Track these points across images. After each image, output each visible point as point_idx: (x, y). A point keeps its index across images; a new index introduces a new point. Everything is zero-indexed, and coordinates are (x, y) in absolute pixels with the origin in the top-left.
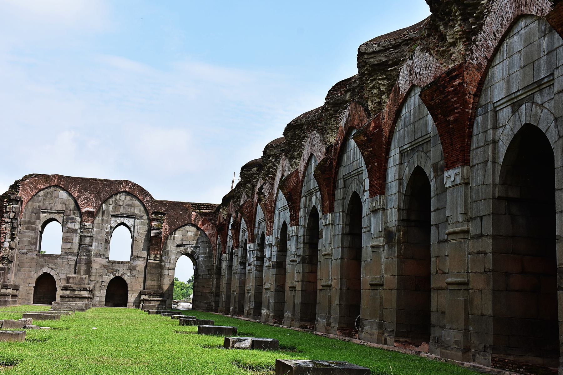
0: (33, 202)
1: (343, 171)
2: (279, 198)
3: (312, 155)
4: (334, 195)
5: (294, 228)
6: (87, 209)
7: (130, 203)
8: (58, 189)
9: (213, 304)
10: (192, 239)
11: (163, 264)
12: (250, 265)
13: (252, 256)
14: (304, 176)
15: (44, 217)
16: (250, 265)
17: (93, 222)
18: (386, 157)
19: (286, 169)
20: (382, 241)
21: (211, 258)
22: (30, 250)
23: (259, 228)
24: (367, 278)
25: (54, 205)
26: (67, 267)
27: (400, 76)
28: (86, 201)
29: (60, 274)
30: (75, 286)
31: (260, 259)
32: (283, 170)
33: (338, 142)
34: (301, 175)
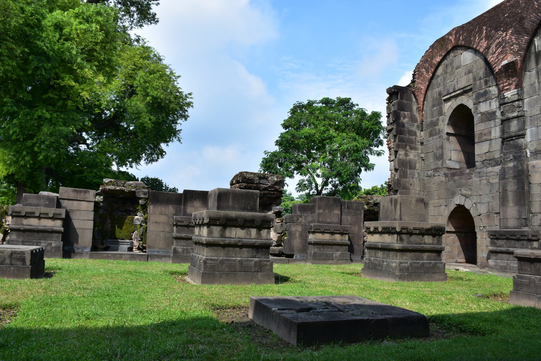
0: (433, 89)
8: (460, 52)
17: (519, 86)
22: (436, 170)
25: (457, 82)
28: (499, 50)
29: (478, 205)
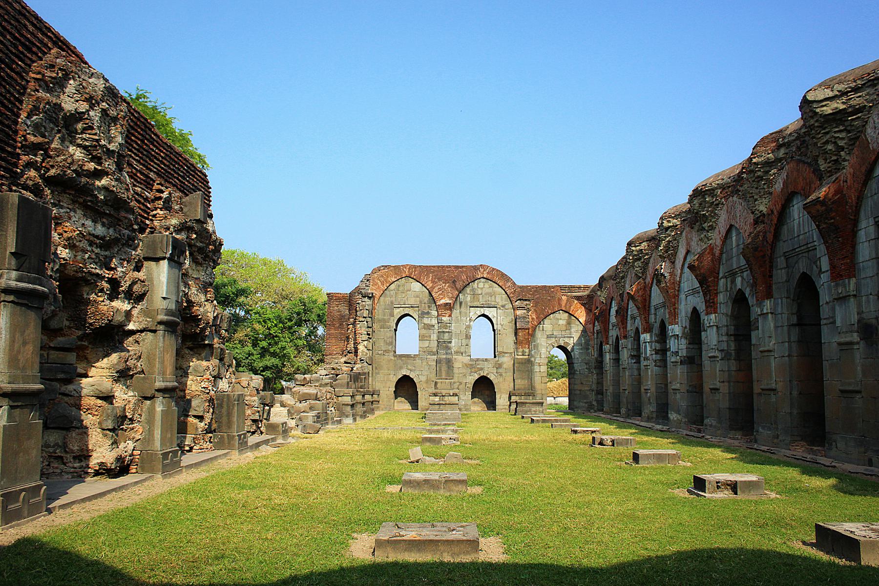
1: (783, 247)
2: (684, 279)
3: (731, 226)
4: (771, 276)
5: (713, 316)
6: (442, 301)
7: (490, 290)
9: (594, 403)
10: (564, 328)
11: (533, 359)
12: (646, 359)
13: (648, 349)
14: (721, 254)
15: (398, 313)
16: (646, 359)
17: (450, 316)
18: (853, 230)
19: (693, 244)
20: (855, 337)
21: (588, 349)
23: (655, 314)
24: (832, 383)
26: (427, 368)
27: (867, 127)
30: (444, 392)
31: (663, 351)
32: (688, 244)
33: (772, 211)
34: (717, 253)
